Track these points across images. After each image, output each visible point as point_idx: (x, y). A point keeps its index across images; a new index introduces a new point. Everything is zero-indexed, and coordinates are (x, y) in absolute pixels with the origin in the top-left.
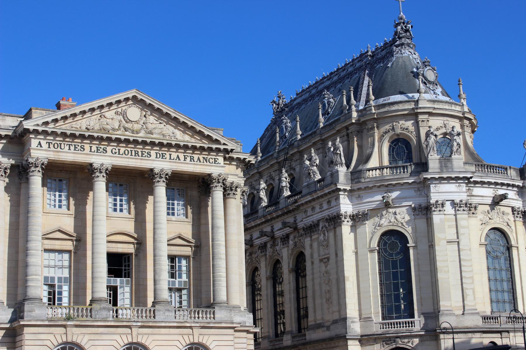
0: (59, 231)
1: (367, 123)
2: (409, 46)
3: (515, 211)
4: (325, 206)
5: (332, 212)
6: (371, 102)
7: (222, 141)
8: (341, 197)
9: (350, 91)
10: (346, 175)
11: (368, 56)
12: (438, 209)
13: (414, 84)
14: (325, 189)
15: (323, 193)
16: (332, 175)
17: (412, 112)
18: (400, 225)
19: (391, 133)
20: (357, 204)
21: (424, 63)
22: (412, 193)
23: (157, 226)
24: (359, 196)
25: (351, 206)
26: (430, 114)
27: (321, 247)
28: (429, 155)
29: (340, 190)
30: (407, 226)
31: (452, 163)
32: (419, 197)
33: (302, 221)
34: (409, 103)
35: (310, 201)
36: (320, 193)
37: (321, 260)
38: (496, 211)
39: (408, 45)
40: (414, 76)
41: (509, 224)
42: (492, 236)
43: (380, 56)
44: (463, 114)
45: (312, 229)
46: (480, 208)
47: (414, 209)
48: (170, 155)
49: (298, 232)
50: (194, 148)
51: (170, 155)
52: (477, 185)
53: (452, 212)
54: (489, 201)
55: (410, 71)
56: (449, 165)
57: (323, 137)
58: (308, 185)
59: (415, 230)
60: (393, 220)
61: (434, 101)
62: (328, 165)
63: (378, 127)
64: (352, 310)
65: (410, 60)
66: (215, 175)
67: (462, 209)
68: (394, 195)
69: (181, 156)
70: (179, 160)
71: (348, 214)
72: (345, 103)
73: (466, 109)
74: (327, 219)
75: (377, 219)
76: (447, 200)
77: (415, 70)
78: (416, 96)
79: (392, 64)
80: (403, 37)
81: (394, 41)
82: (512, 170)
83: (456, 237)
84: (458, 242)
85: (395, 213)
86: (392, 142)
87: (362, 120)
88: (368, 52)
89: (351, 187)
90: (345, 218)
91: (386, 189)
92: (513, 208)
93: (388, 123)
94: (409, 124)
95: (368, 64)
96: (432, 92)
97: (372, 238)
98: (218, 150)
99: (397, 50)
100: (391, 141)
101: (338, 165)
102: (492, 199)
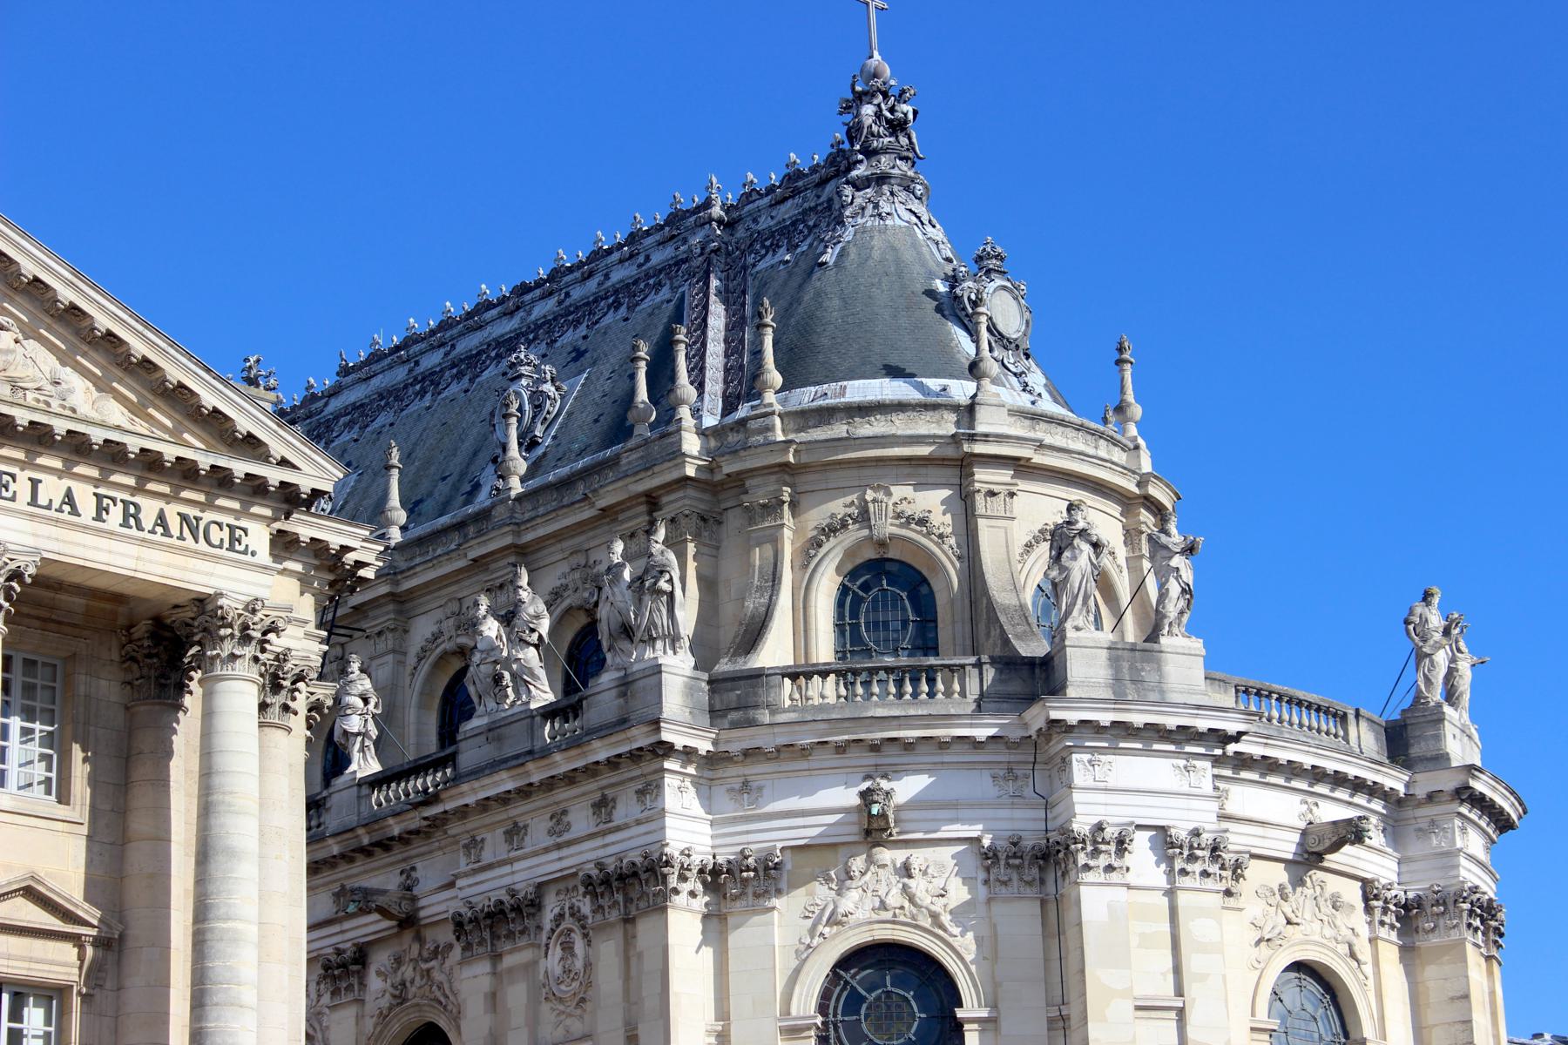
1: (748, 483)
2: (907, 189)
3: (1376, 897)
4: (581, 820)
5: (622, 847)
6: (770, 397)
7: (277, 449)
8: (670, 782)
9: (635, 360)
10: (690, 690)
11: (711, 220)
12: (1103, 861)
14: (596, 744)
15: (579, 764)
16: (625, 685)
17: (950, 452)
18: (926, 922)
19: (854, 534)
20: (735, 821)
21: (979, 259)
22: (980, 784)
24: (746, 784)
25: (707, 829)
26: (1022, 467)
27: (545, 1007)
28: (1068, 625)
29: (667, 749)
30: (956, 931)
31: (1159, 669)
32: (1013, 806)
33: (451, 885)
34: (936, 415)
35: (504, 799)
36: (562, 763)
38: (1309, 892)
40: (939, 309)
41: (1356, 949)
42: (1291, 996)
43: (765, 223)
44: (1139, 485)
46: (1254, 870)
47: (990, 857)
48: (35, 483)
49: (419, 938)
50: (150, 464)
51: (35, 483)
52: (1244, 775)
53: (1157, 876)
54: (1287, 846)
55: (919, 288)
56: (1149, 676)
57: (529, 537)
58: (491, 728)
59: (990, 948)
60: (895, 898)
63: (794, 505)
65: (915, 244)
66: (231, 604)
67: (1197, 867)
68: (906, 788)
69: (85, 496)
70: (74, 511)
71: (696, 860)
72: (642, 394)
73: (1146, 466)
74: (588, 882)
75: (822, 892)
76: (1139, 827)
77: (941, 287)
78: (961, 390)
79: (841, 255)
80: (885, 150)
81: (839, 164)
82: (1363, 724)
83: (1169, 989)
84: (1181, 1012)
85: (906, 870)
86: (853, 575)
87: (729, 467)
88: (707, 204)
89: (715, 743)
90: (683, 878)
91: (871, 759)
92: (1366, 884)
93: (842, 490)
94: (933, 502)
95: (716, 251)
96: (1014, 380)
97: (797, 972)
98: (255, 488)
99: (858, 201)
100: (849, 567)
101: (659, 644)
102: (1296, 837)
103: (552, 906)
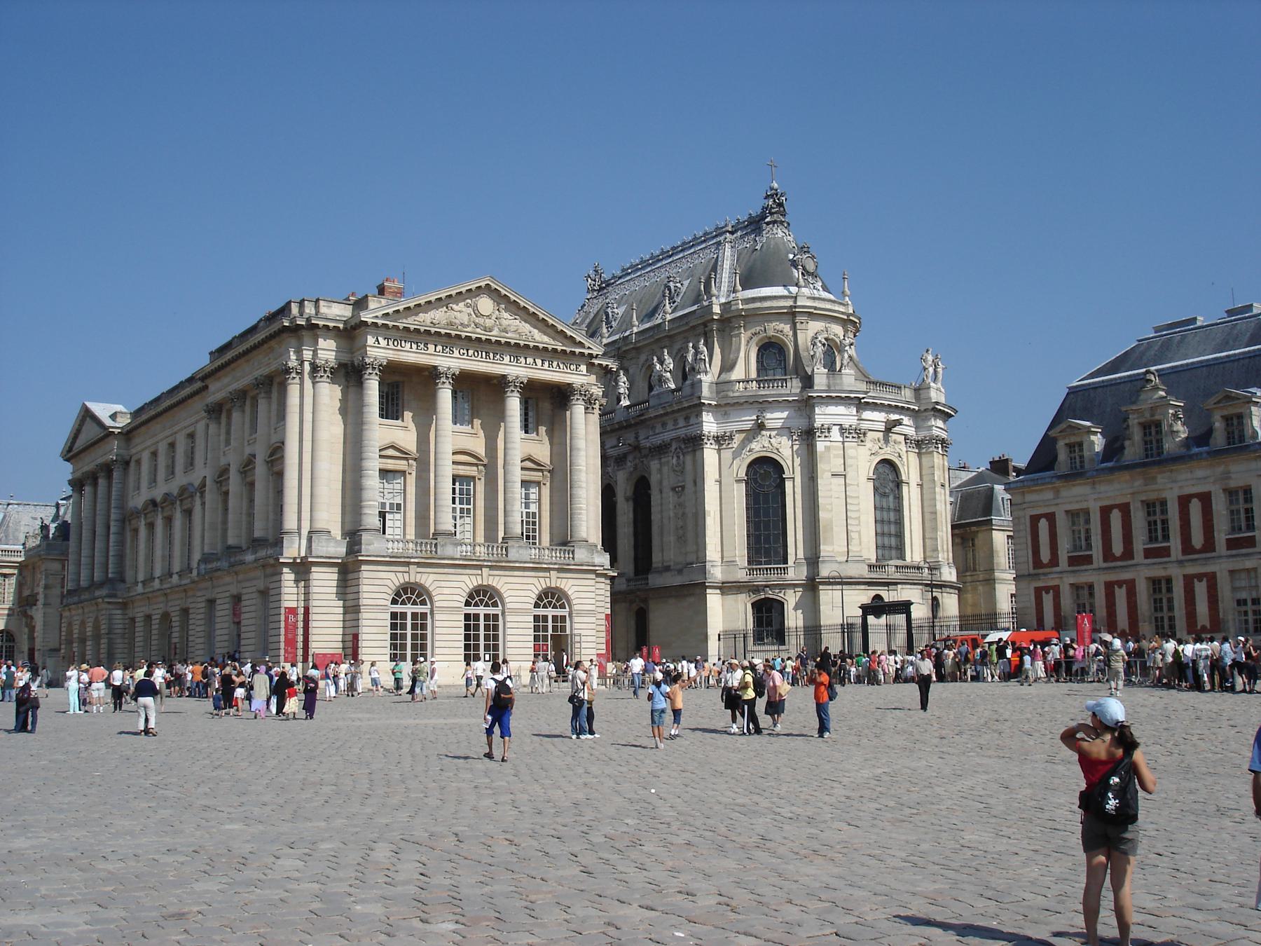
0: (393, 447)
5: (691, 431)
7: (587, 345)
13: (792, 276)
23: (509, 446)
35: (661, 415)
37: (673, 489)
39: (782, 222)
45: (661, 450)
46: (870, 434)
50: (555, 350)
61: (814, 298)
62: (686, 374)
64: (712, 552)
78: (794, 289)
87: (726, 316)
98: (582, 354)
103: (674, 446)
